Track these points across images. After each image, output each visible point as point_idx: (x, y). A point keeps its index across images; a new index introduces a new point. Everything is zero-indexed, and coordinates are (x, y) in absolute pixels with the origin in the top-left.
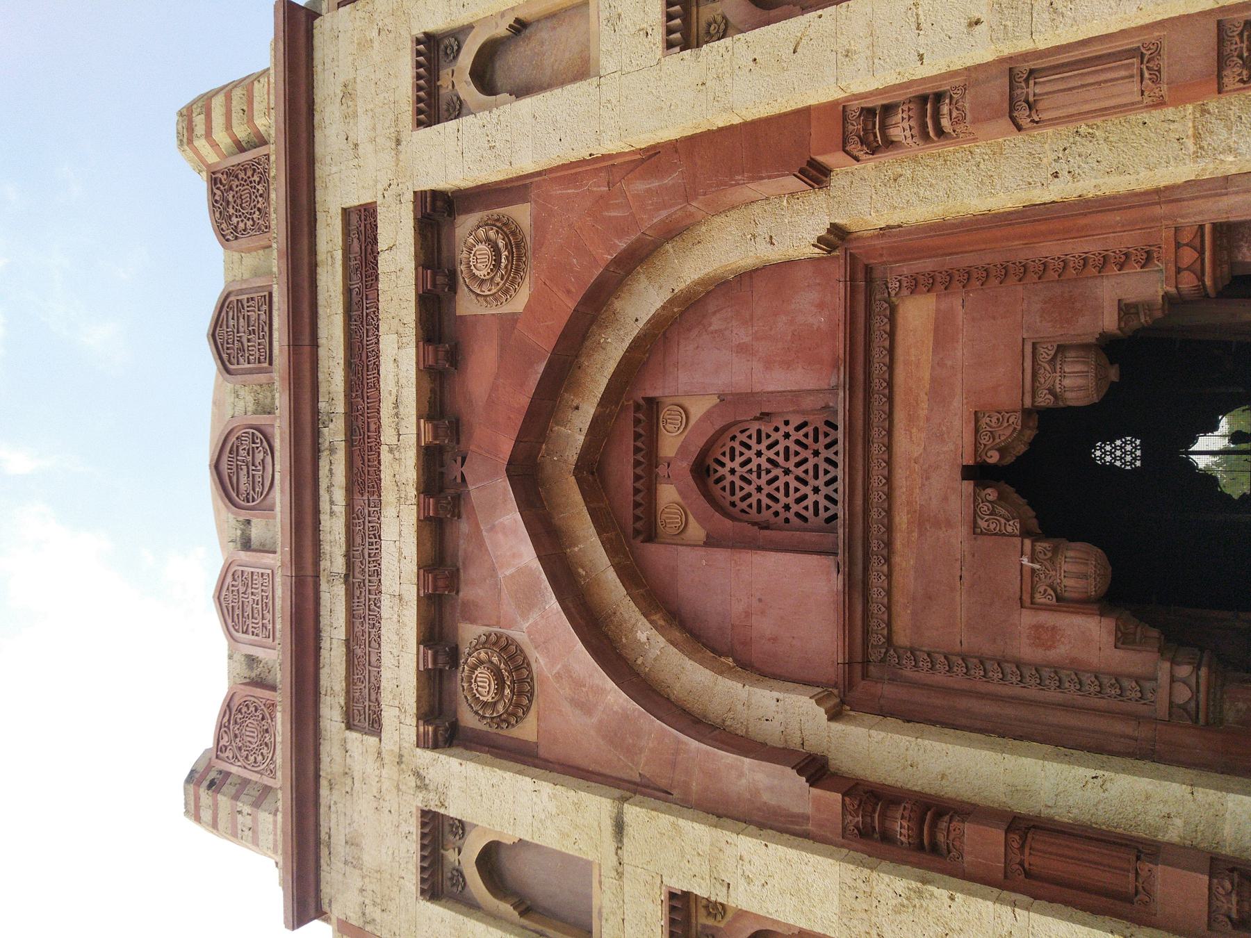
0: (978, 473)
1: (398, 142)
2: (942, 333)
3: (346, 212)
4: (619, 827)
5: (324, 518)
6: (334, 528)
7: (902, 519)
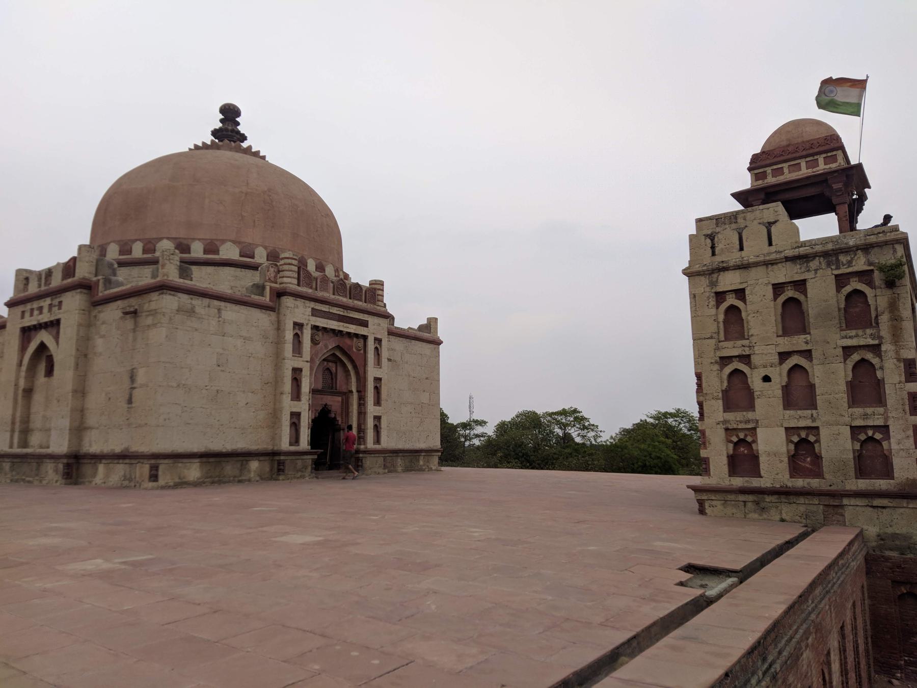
0: (326, 405)
1: (374, 334)
2: (338, 402)
3: (368, 321)
4: (307, 362)
5: (336, 308)
6: (335, 310)
7: (322, 396)
